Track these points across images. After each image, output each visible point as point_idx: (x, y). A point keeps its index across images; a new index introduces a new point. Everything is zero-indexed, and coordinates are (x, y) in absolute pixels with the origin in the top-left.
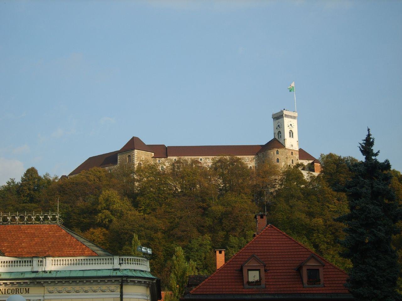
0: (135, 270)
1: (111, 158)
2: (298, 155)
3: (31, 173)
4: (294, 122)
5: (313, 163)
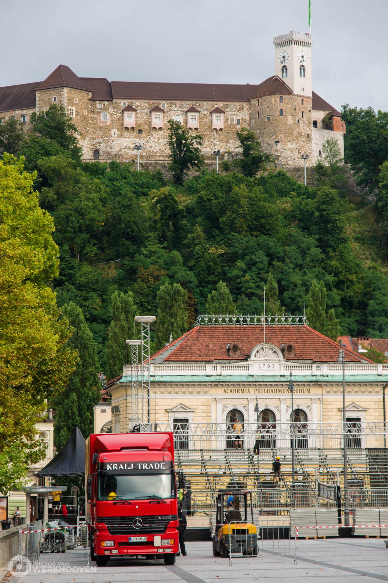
2: (311, 104)
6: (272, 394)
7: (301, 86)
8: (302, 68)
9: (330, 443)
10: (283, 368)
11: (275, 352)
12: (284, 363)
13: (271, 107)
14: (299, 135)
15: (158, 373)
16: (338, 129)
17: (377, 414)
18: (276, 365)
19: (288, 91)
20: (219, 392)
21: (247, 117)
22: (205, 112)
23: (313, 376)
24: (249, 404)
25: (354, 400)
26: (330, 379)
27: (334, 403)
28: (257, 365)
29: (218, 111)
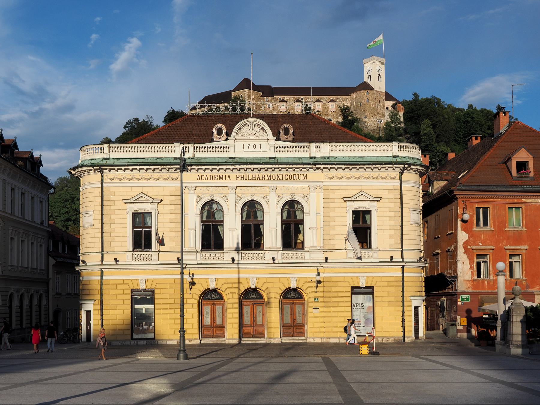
0: (413, 158)
1: (225, 97)
4: (383, 67)
5: (395, 104)
6: (259, 181)
7: (379, 86)
9: (332, 242)
11: (263, 128)
12: (273, 142)
13: (362, 97)
14: (378, 113)
18: (265, 146)
19: (371, 88)
22: (325, 102)
23: (311, 158)
25: (363, 188)
26: (332, 160)
27: (336, 192)
28: (239, 145)
29: (332, 101)
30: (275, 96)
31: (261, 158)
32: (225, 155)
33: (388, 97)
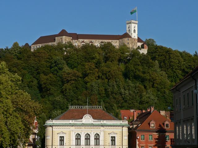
1: (52, 38)
3: (16, 45)
4: (136, 25)
5: (143, 45)
8: (134, 31)
10: (92, 121)
15: (55, 123)
16: (145, 48)
17: (120, 135)
19: (130, 37)
20: (73, 128)
21: (118, 44)
24: (83, 132)
30: (79, 40)
31: (90, 124)
32: (81, 123)
33: (139, 40)
